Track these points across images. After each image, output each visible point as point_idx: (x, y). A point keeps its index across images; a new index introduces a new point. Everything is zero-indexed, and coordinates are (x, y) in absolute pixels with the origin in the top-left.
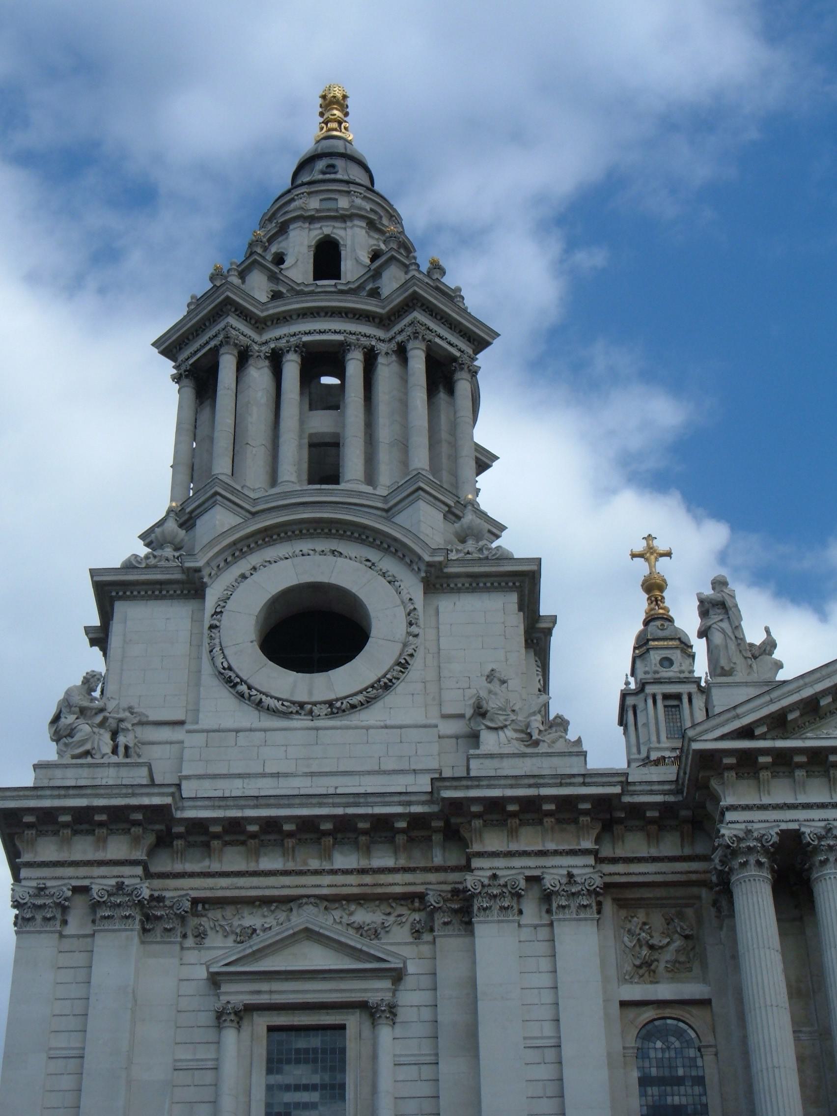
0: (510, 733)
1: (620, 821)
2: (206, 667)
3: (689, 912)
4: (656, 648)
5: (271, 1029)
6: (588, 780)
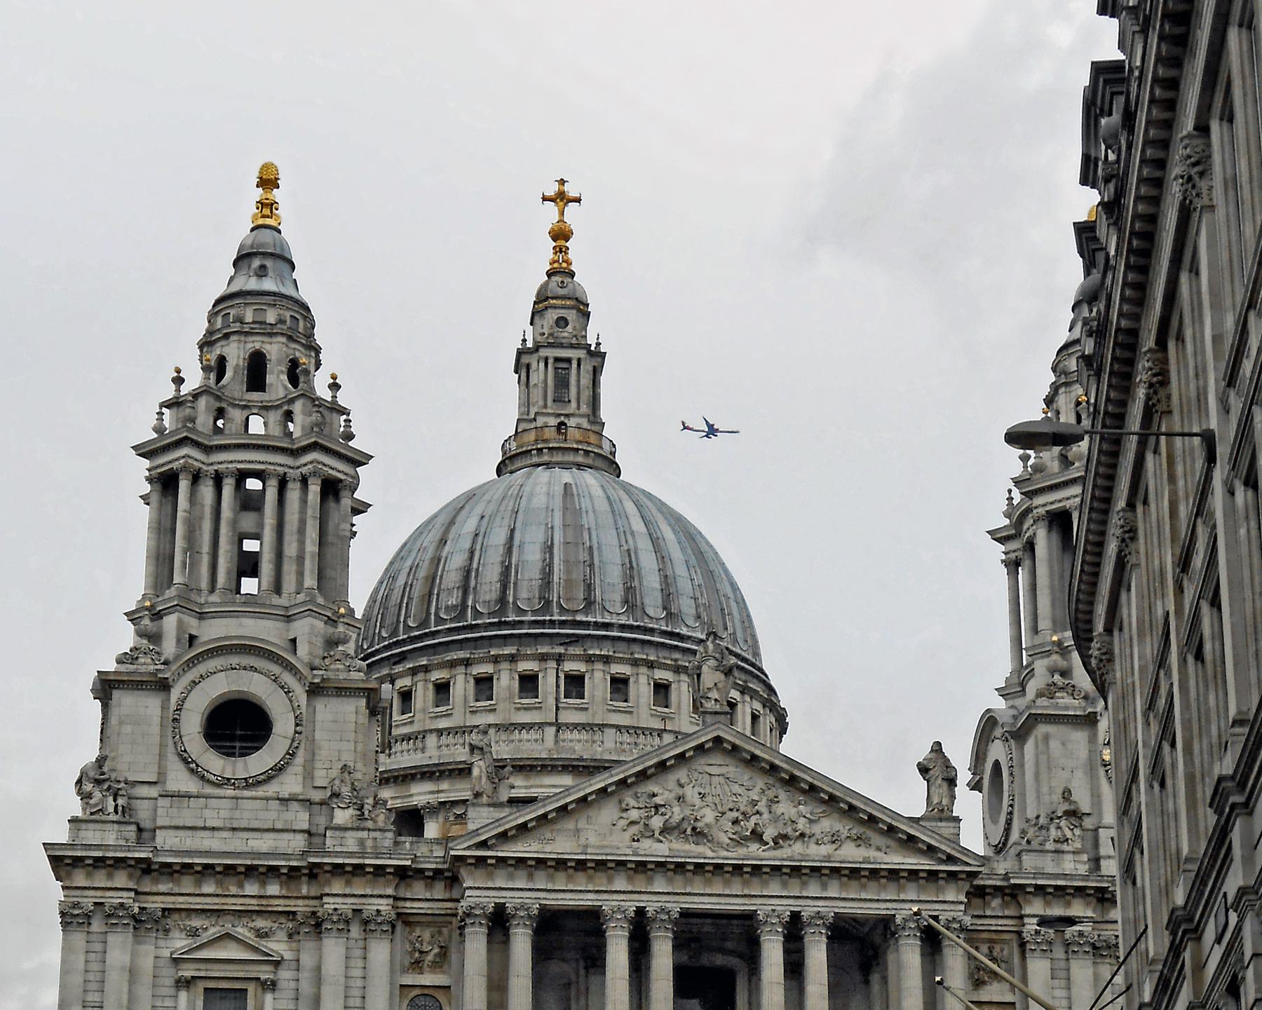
0: (351, 811)
1: (411, 877)
2: (171, 748)
3: (445, 931)
4: (555, 307)
5: (205, 989)
6: (392, 856)
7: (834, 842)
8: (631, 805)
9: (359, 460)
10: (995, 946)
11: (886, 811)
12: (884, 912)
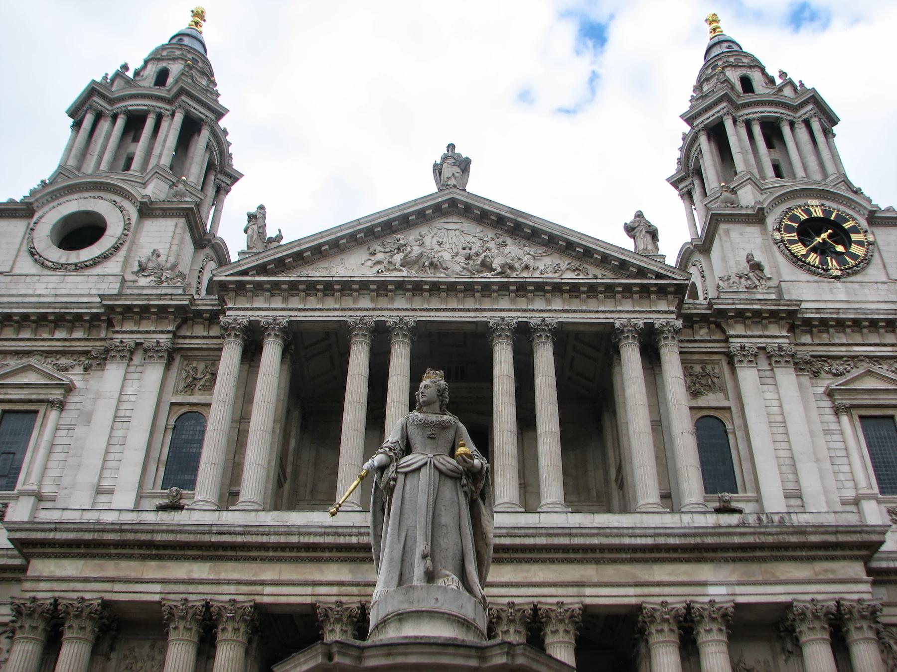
0: (152, 278)
1: (192, 319)
2: (25, 247)
7: (556, 272)
8: (378, 251)
9: (220, 114)
10: (707, 366)
11: (599, 243)
12: (604, 321)
